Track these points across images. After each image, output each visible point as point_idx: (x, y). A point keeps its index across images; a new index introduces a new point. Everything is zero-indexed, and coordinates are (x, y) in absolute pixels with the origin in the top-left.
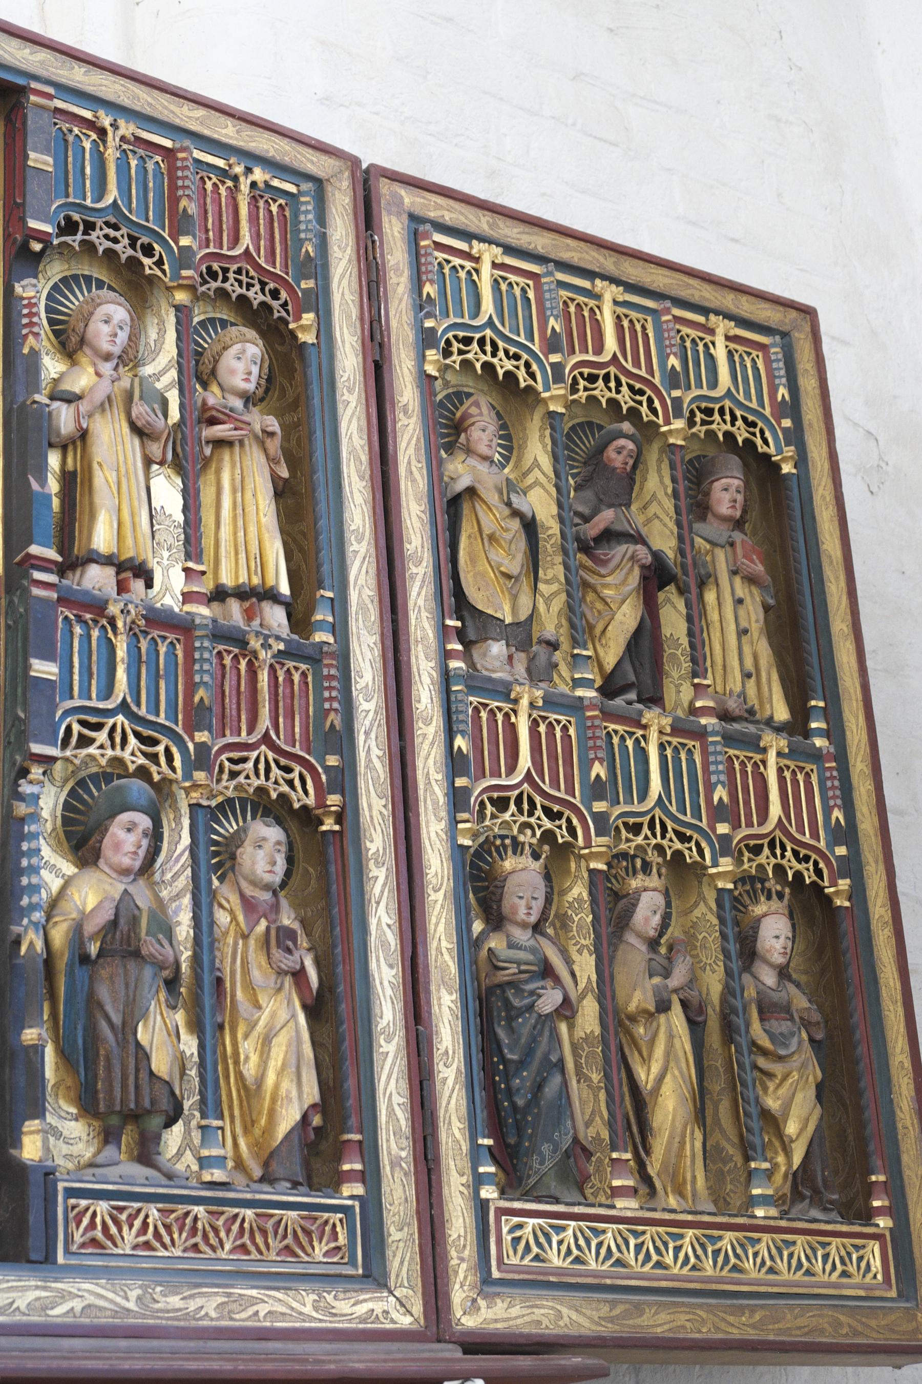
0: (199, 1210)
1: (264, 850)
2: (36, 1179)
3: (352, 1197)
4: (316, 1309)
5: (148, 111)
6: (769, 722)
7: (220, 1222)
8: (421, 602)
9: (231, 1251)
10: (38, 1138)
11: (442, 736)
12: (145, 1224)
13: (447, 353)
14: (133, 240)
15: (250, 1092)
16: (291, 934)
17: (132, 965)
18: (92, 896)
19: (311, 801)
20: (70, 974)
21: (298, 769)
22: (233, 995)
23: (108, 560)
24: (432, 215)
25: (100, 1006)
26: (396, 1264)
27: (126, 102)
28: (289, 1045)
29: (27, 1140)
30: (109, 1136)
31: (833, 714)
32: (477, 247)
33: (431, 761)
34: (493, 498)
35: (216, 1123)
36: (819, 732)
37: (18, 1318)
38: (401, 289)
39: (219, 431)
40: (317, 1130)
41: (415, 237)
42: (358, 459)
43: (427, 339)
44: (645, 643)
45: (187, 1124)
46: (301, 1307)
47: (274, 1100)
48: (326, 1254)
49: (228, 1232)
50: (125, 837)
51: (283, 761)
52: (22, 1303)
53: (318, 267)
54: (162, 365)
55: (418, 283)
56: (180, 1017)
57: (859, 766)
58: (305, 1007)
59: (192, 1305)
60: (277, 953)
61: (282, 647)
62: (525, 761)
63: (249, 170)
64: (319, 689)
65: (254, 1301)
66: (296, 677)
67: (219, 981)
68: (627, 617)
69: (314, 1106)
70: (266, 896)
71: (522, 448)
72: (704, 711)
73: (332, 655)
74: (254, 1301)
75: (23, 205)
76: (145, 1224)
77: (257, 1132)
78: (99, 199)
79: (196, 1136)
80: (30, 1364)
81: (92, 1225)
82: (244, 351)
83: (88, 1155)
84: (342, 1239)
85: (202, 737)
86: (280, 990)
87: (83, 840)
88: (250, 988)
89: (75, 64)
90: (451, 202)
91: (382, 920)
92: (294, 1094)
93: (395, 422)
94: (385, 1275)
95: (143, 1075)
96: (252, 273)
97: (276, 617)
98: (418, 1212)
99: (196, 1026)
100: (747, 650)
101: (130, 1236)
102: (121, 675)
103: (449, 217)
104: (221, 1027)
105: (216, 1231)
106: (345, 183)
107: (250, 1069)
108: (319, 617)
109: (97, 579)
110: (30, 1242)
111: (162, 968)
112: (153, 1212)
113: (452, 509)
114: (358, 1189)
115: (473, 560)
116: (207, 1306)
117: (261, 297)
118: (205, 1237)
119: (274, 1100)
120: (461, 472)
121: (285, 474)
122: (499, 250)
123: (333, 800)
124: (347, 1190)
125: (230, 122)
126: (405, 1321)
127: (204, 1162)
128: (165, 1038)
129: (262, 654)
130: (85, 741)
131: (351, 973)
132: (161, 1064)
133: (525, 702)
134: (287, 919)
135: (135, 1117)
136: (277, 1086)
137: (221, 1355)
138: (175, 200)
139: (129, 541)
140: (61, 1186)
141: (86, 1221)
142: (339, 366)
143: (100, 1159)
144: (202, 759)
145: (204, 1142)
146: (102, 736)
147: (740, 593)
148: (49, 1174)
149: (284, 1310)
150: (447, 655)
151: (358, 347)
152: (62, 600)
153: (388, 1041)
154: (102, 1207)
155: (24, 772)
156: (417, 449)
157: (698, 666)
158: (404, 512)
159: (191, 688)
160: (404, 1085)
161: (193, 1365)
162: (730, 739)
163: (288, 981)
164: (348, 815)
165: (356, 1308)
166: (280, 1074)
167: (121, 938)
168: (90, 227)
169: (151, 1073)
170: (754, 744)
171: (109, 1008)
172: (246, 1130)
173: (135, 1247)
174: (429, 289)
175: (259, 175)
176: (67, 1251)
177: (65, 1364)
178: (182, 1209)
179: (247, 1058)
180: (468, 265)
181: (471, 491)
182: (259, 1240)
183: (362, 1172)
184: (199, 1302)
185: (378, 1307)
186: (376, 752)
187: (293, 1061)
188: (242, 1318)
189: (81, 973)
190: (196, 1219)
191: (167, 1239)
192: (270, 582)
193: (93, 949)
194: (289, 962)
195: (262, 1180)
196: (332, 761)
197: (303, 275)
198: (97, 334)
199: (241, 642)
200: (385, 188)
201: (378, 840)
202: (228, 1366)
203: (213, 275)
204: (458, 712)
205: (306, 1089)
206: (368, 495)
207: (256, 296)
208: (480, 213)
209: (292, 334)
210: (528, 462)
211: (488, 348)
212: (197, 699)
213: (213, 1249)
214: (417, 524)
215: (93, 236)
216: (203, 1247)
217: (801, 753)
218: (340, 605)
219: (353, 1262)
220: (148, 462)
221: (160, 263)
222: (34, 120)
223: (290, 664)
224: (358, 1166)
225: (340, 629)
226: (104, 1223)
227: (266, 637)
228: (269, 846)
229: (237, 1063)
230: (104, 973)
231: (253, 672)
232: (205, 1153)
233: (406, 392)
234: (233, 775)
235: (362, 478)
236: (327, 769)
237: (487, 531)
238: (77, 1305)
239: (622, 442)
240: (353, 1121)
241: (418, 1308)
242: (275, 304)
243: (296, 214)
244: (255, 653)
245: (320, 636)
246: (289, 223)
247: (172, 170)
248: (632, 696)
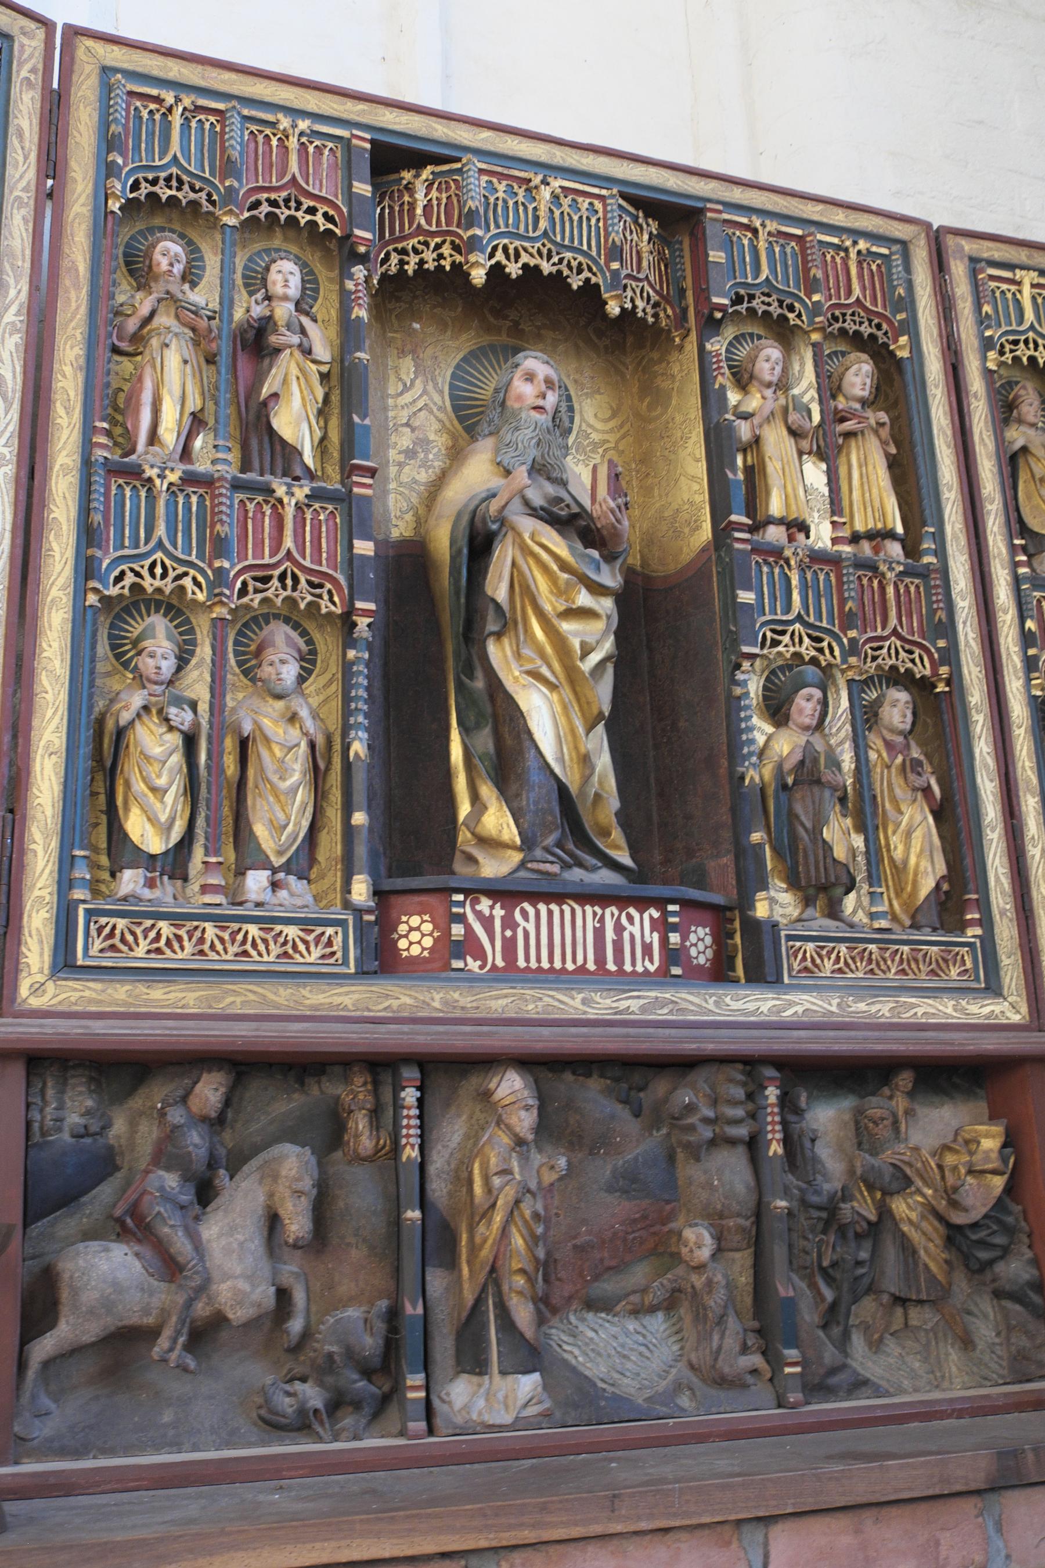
0: (872, 947)
1: (897, 708)
2: (766, 929)
3: (974, 936)
4: (955, 1010)
5: (785, 211)
7: (887, 955)
8: (995, 529)
9: (896, 973)
10: (766, 903)
11: (1016, 620)
12: (838, 958)
13: (1002, 353)
14: (781, 303)
15: (899, 870)
16: (920, 763)
17: (816, 789)
18: (786, 745)
19: (928, 672)
20: (777, 798)
21: (917, 651)
22: (883, 806)
23: (781, 521)
24: (985, 255)
25: (797, 817)
26: (1007, 980)
27: (769, 207)
28: (924, 837)
29: (758, 905)
30: (807, 902)
32: (1019, 274)
33: (1010, 639)
35: (879, 890)
37: (762, 1018)
38: (966, 311)
39: (848, 426)
40: (946, 893)
41: (974, 273)
42: (944, 433)
43: (987, 344)
45: (858, 892)
46: (945, 1009)
47: (916, 874)
48: (959, 974)
49: (893, 961)
50: (805, 705)
51: (907, 647)
52: (764, 1008)
53: (908, 304)
54: (805, 385)
55: (978, 306)
56: (849, 821)
58: (932, 812)
59: (874, 1009)
60: (912, 777)
61: (901, 568)
63: (855, 243)
64: (929, 595)
65: (914, 1006)
66: (912, 589)
67: (874, 797)
69: (943, 877)
70: (900, 739)
73: (936, 571)
74: (914, 1006)
75: (708, 288)
76: (838, 958)
77: (905, 896)
78: (756, 277)
79: (866, 901)
80: (776, 1047)
81: (804, 958)
82: (860, 369)
83: (796, 914)
84: (969, 964)
85: (853, 634)
86: (915, 801)
87: (777, 710)
88: (894, 801)
89: (734, 187)
90: (999, 245)
91: (983, 749)
92: (930, 869)
93: (969, 406)
94: (1000, 987)
95: (829, 861)
96: (862, 314)
97: (895, 549)
98: (1020, 945)
99: (861, 827)
101: (828, 965)
102: (796, 596)
103: (997, 256)
104: (877, 828)
105: (885, 960)
106: (922, 242)
107: (898, 854)
108: (925, 546)
109: (775, 534)
110: (767, 970)
111: (836, 790)
112: (843, 948)
113: (1013, 462)
114: (978, 931)
115: (1029, 498)
116: (883, 1009)
117: (869, 330)
118: (878, 964)
119: (916, 874)
120: (1017, 436)
121: (893, 450)
122: (1036, 274)
123: (944, 670)
124: (970, 932)
125: (840, 211)
126: (1016, 1018)
127: (873, 916)
128: (842, 837)
129: (889, 575)
130: (775, 643)
131: (964, 787)
132: (840, 853)
134: (916, 753)
135: (824, 888)
136: (917, 865)
137: (897, 1040)
138: (807, 271)
139: (794, 507)
140: (783, 933)
141: (800, 956)
142: (927, 370)
143: (805, 916)
144: (853, 648)
145: (872, 904)
146: (786, 639)
148: (775, 925)
149: (933, 1011)
150: (1016, 565)
151: (940, 356)
152: (754, 551)
153: (993, 831)
154: (810, 946)
155: (738, 666)
156: (986, 422)
158: (980, 468)
159: (843, 601)
160: (1005, 860)
161: (879, 1047)
163: (919, 795)
164: (955, 680)
165: (982, 1010)
166: (919, 856)
167: (809, 773)
168: (752, 297)
169: (834, 860)
171: (803, 818)
172: (898, 895)
173: (833, 972)
174: (987, 308)
175: (862, 245)
176: (790, 976)
177: (797, 1047)
178: (862, 946)
179: (896, 848)
180: (1013, 288)
181: (1024, 449)
182: (913, 966)
183: (980, 920)
184: (878, 1007)
185: (997, 1009)
186: (971, 635)
187: (927, 848)
188: (906, 1017)
189: (783, 796)
190: (871, 953)
191: (853, 967)
192: (890, 526)
193: (790, 780)
194: (919, 782)
195: (911, 927)
196: (941, 643)
197: (897, 310)
198: (762, 370)
199: (874, 568)
200: (950, 241)
201: (976, 695)
202: (902, 1048)
203: (836, 319)
204: (1027, 603)
205: (937, 866)
206: (953, 458)
207: (866, 330)
208: (1020, 249)
209: (892, 354)
211: (1031, 346)
212: (847, 609)
213: (884, 972)
214: (989, 475)
215: (754, 303)
216: (877, 971)
218: (940, 537)
219: (977, 979)
220: (800, 453)
221: (799, 316)
222: (710, 230)
223: (908, 580)
224: (977, 916)
225: (941, 552)
226: (812, 957)
227: (891, 563)
228: (901, 705)
229: (889, 850)
230: (798, 796)
231: (882, 588)
232: (874, 909)
233: (976, 384)
234: (874, 658)
235: (949, 447)
236: (938, 649)
238: (800, 1009)
240: (971, 886)
241: (1024, 1009)
242: (880, 334)
243: (889, 268)
244: (883, 575)
245: (927, 559)
246: (885, 276)
247: (803, 250)
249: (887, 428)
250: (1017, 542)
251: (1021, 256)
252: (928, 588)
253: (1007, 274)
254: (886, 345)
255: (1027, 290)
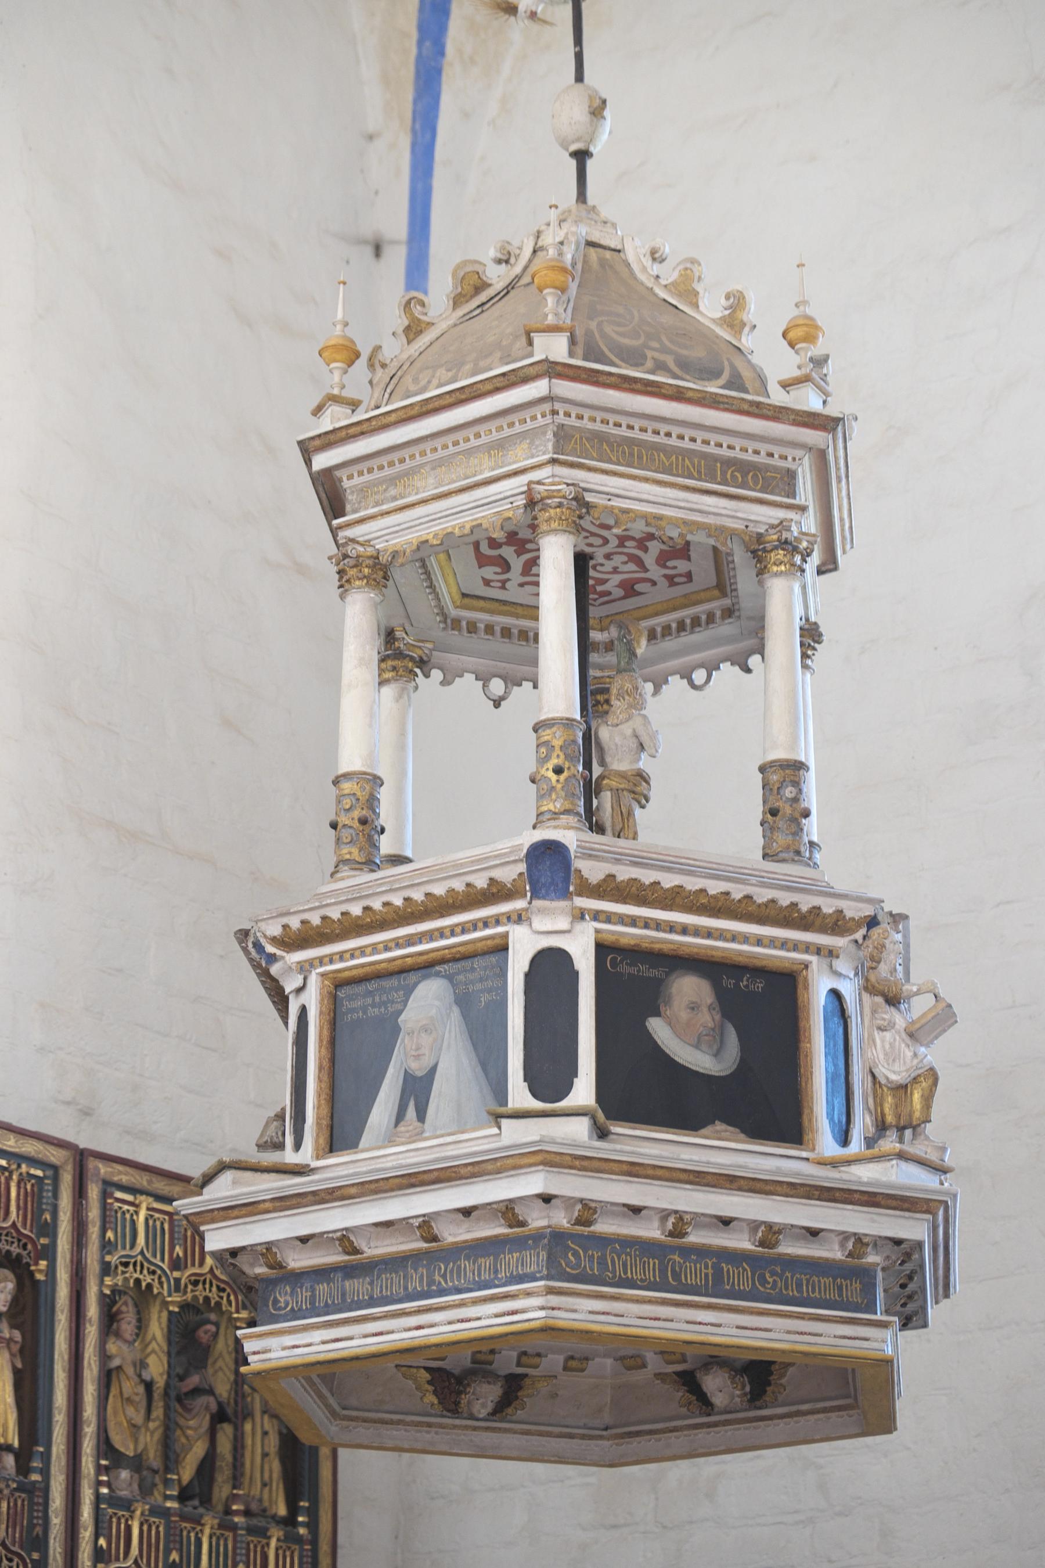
6: (274, 1517)
11: (93, 1537)
21: (16, 1560)
24: (116, 1179)
31: (313, 1513)
33: (86, 1555)
34: (130, 1371)
36: (302, 1524)
41: (105, 1195)
42: (63, 1358)
43: (106, 1269)
44: (207, 1467)
51: (9, 1555)
53: (50, 1230)
55: (104, 1230)
57: (324, 1547)
61: (15, 1485)
62: (135, 1550)
63: (19, 1166)
64: (31, 1511)
66: (19, 1503)
68: (199, 1450)
71: (147, 1326)
72: (237, 1513)
73: (39, 1489)
90: (128, 1169)
96: (14, 1234)
100: (266, 1467)
103: (124, 1179)
106: (69, 1167)
108: (35, 1465)
115: (115, 1413)
117: (18, 1251)
121: (19, 1365)
133: (138, 1513)
142: (57, 1295)
147: (267, 1426)
151: (68, 1280)
157: (236, 1480)
162: (251, 1530)
170: (263, 1533)
174: (110, 1234)
180: (132, 1209)
181: (119, 1368)
186: (59, 1550)
192: (10, 1442)
196: (35, 1556)
197: (40, 1234)
200: (92, 1164)
204: (103, 1522)
206: (66, 1382)
208: (143, 1173)
210: (149, 1337)
217: (291, 1539)
218: (46, 1457)
223: (17, 1494)
225: (45, 1472)
235: (64, 1371)
236: (32, 1560)
237: (126, 1396)
239: (209, 1327)
242: (25, 1253)
243: (41, 1190)
245: (35, 1477)
246: (37, 1195)
248: (196, 1502)
249: (18, 1346)
250: (103, 1462)
251: (142, 1180)
252: (32, 1503)
253: (129, 1197)
254: (28, 1265)
255: (143, 1213)
